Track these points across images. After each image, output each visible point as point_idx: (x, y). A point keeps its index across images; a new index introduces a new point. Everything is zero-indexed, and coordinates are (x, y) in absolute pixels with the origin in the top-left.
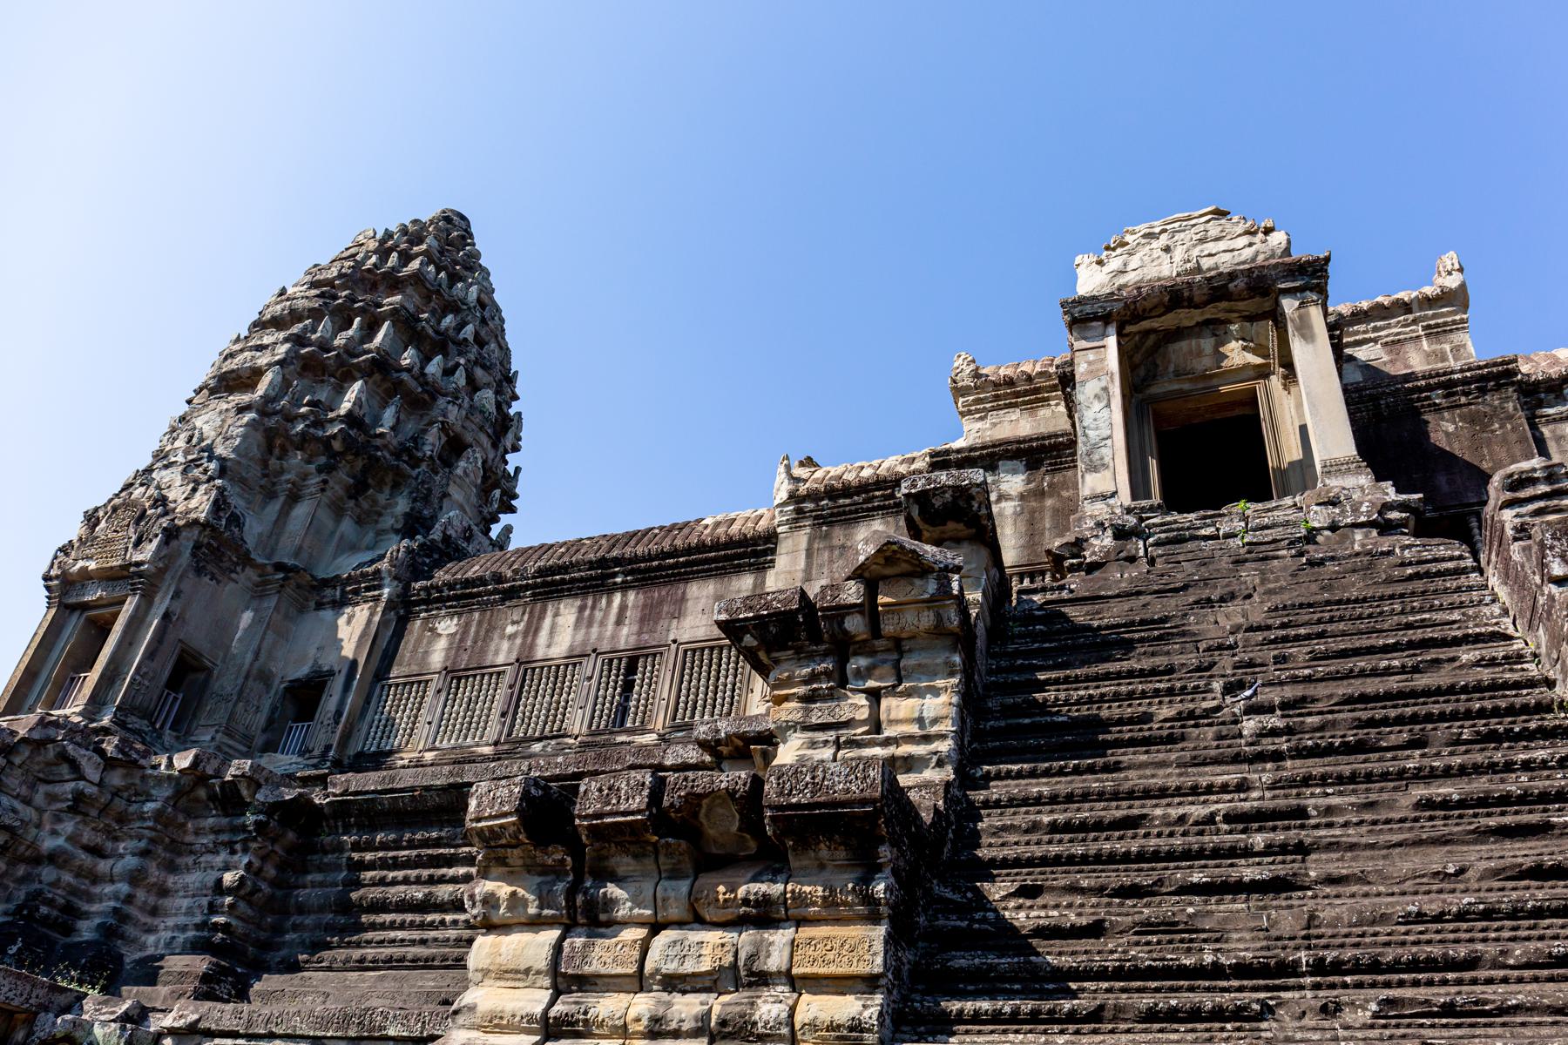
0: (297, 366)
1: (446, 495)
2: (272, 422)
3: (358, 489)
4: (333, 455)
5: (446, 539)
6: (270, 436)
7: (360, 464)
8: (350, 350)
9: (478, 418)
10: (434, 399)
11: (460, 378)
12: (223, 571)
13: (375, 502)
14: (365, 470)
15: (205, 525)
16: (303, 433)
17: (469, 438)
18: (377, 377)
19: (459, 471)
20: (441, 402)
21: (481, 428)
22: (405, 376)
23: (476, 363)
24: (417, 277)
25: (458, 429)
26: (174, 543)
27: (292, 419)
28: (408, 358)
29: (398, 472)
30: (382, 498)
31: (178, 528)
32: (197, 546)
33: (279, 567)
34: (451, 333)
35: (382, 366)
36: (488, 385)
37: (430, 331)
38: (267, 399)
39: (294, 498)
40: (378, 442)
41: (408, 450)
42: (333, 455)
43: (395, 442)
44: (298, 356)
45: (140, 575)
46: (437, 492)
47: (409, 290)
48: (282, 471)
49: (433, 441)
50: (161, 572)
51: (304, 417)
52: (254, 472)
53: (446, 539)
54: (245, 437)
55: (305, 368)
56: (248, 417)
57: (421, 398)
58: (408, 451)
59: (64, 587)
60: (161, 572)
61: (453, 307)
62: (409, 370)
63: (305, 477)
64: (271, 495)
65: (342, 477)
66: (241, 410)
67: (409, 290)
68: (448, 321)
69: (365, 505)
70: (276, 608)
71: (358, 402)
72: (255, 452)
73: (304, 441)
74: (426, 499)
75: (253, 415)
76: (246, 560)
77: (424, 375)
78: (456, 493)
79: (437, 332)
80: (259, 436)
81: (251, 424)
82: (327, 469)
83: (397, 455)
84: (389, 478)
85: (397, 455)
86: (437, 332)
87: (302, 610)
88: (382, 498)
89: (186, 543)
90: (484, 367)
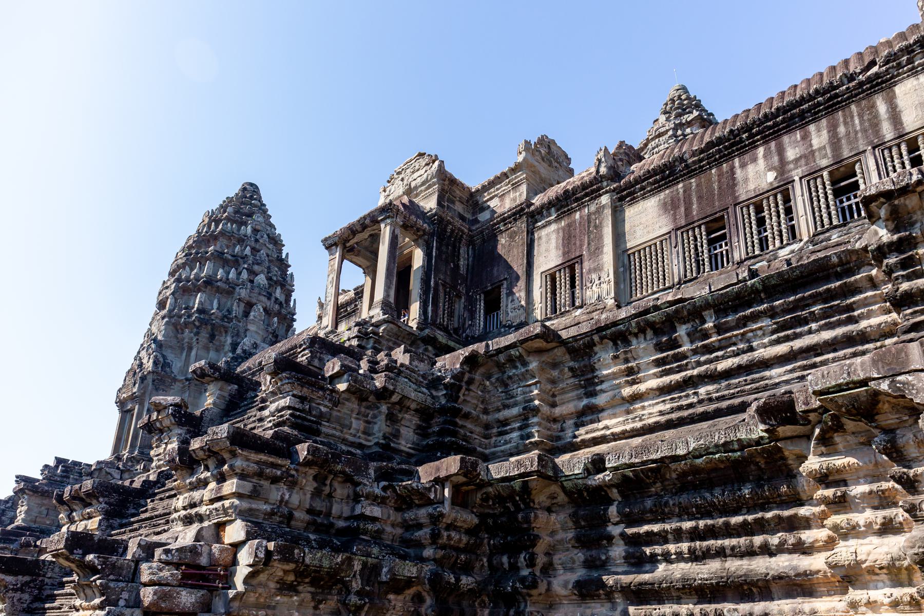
0: (181, 291)
1: (246, 330)
2: (173, 320)
3: (212, 337)
4: (198, 328)
5: (244, 351)
6: (175, 325)
7: (209, 327)
8: (197, 279)
9: (257, 290)
10: (234, 289)
11: (245, 275)
12: (167, 387)
13: (220, 341)
14: (212, 330)
15: (153, 372)
16: (185, 322)
17: (254, 301)
18: (209, 287)
19: (251, 317)
20: (237, 289)
21: (260, 294)
22: (219, 284)
23: (253, 264)
24: (222, 233)
25: (247, 298)
26: (145, 382)
27: (180, 317)
28: (220, 274)
29: (224, 327)
30: (222, 339)
31: (145, 376)
32: (153, 381)
33: (187, 379)
34: (240, 254)
35: (210, 282)
36: (262, 272)
37: (230, 257)
38: (170, 311)
39: (190, 349)
40: (213, 317)
41: (225, 316)
42: (198, 328)
43: (220, 314)
44: (179, 288)
45: (136, 397)
46: (242, 330)
47: (221, 239)
48: (183, 339)
49: (237, 310)
50: (144, 394)
51: (184, 314)
52: (174, 342)
53: (244, 351)
54: (165, 329)
55: (184, 291)
56: (166, 319)
57: (229, 289)
58: (227, 317)
59: (121, 404)
60: (144, 394)
61: (241, 241)
62: (221, 280)
63: (192, 339)
64: (183, 349)
65: (204, 334)
66: (163, 318)
67: (221, 239)
68: (238, 248)
69: (217, 343)
70: (189, 396)
71: (201, 303)
72: (171, 334)
73: (186, 324)
74: (238, 335)
75: (166, 319)
76: (175, 380)
77: (228, 279)
78: (252, 328)
79: (233, 256)
80: (171, 327)
81: (167, 323)
82: (197, 334)
83: (222, 320)
84: (222, 330)
85: (222, 320)
86: (233, 256)
87: (201, 393)
88: (222, 339)
89: (150, 378)
90: (258, 264)
